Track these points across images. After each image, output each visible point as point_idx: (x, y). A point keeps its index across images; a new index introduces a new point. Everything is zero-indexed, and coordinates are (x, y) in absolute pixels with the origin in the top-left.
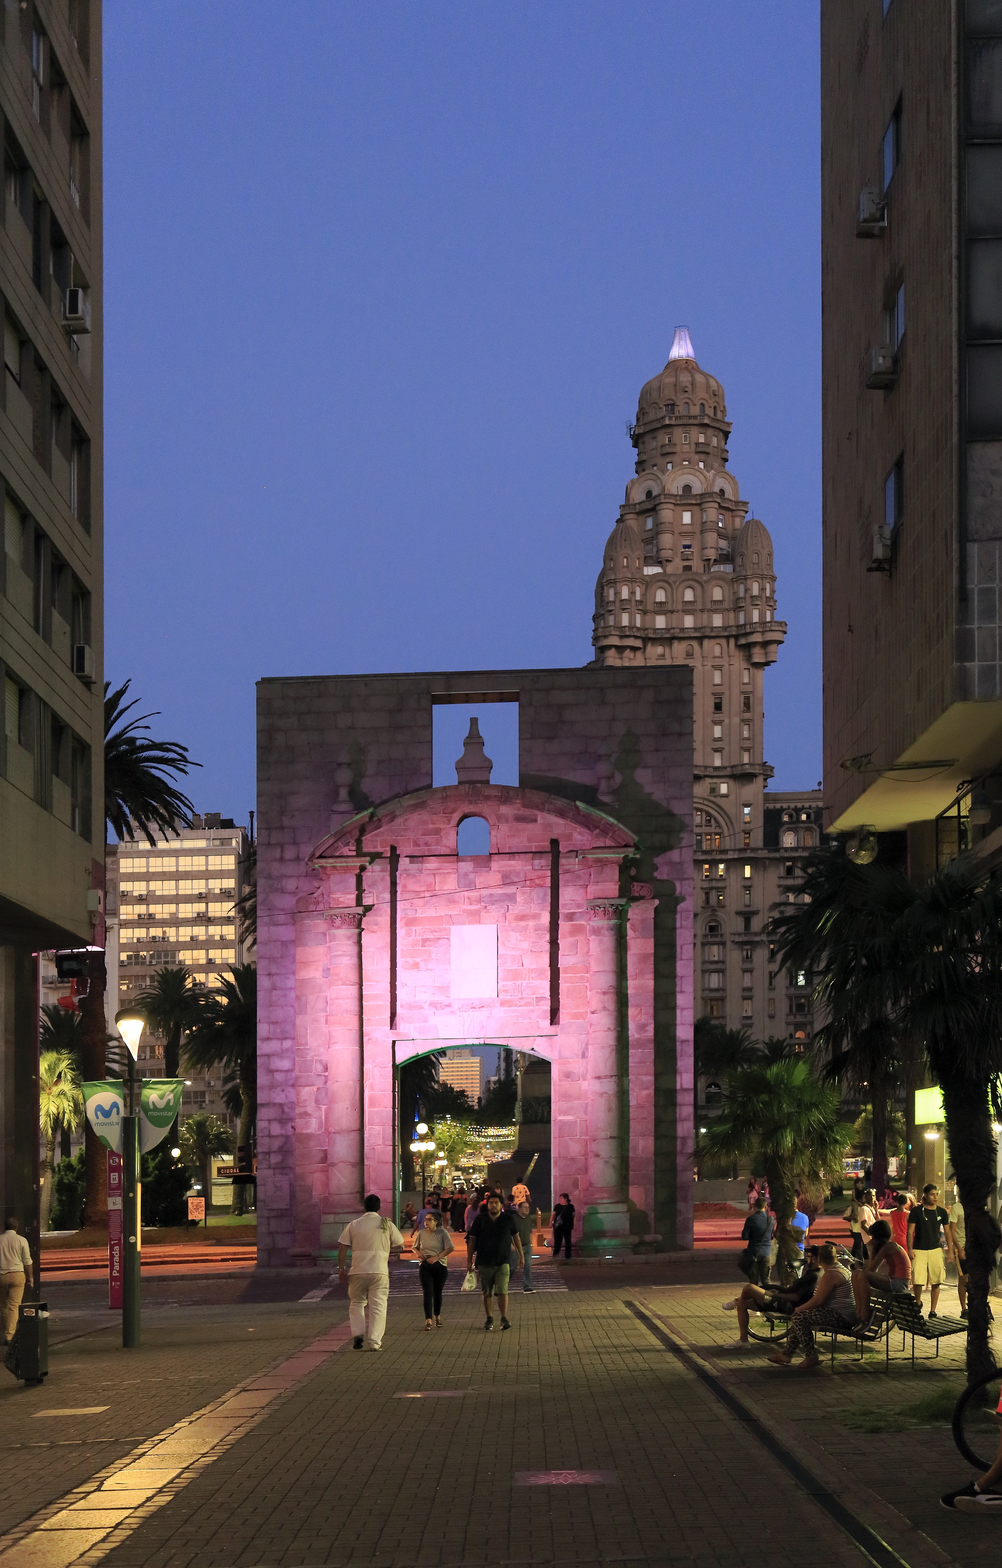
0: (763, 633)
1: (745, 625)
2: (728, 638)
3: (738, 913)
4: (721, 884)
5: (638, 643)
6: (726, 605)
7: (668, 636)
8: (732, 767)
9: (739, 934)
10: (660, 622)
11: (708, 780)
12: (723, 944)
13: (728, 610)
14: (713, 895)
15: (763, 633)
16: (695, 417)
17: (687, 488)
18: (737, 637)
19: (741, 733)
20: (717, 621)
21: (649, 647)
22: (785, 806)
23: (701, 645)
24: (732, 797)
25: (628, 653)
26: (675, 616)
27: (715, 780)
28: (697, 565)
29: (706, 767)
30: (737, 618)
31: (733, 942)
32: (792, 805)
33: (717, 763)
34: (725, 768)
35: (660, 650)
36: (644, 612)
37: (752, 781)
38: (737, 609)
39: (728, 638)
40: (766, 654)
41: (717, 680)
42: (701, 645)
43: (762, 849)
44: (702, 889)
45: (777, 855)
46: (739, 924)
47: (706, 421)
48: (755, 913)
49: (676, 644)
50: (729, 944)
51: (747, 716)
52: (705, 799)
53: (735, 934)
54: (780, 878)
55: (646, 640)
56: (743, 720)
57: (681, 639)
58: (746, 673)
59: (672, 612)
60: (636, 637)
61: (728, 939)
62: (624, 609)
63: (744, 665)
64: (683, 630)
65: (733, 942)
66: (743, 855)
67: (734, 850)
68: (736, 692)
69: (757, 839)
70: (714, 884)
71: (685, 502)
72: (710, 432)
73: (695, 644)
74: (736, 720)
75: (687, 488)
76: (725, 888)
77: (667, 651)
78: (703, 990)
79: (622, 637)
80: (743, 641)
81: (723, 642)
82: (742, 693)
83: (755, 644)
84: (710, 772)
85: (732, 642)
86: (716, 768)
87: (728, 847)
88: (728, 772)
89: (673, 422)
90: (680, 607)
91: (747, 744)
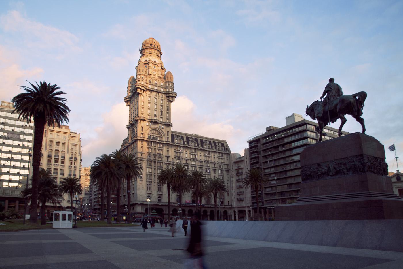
0: (172, 94)
1: (168, 92)
2: (164, 94)
3: (166, 156)
4: (162, 149)
5: (145, 89)
6: (164, 87)
7: (152, 90)
8: (165, 122)
9: (166, 161)
10: (150, 86)
11: (159, 124)
12: (162, 163)
13: (164, 88)
14: (160, 151)
15: (172, 94)
16: (157, 48)
17: (155, 61)
18: (166, 94)
19: (166, 115)
20: (162, 89)
21: (147, 91)
22: (175, 134)
23: (158, 94)
24: (165, 129)
25: (142, 91)
26: (153, 86)
27: (161, 125)
28: (157, 77)
29: (159, 121)
30: (166, 90)
31: (164, 163)
32: (176, 134)
33: (161, 121)
34: (163, 122)
35: (149, 93)
36: (146, 83)
37: (169, 127)
38: (166, 88)
39: (164, 94)
40: (173, 99)
41: (162, 103)
42: (158, 94)
43: (171, 142)
44: (158, 149)
45: (174, 144)
46: (166, 159)
47: (159, 50)
48: (170, 157)
49: (153, 92)
50: (163, 163)
51: (168, 112)
52: (158, 128)
53: (165, 161)
54: (175, 150)
55: (147, 89)
56: (167, 113)
57: (154, 91)
58: (168, 103)
59: (152, 85)
60: (145, 88)
61: (163, 162)
62: (142, 81)
63: (167, 101)
64: (155, 89)
65: (164, 163)
66: (167, 143)
67: (165, 141)
68: (166, 106)
69: (170, 140)
70: (160, 148)
71: (155, 63)
72: (159, 52)
73: (157, 93)
74: (166, 112)
75: (155, 61)
76: (162, 150)
77: (151, 93)
78: (158, 173)
79: (142, 87)
80: (168, 95)
81: (163, 95)
82: (167, 106)
83: (170, 96)
84: (160, 122)
85: (165, 95)
86: (161, 122)
87: (163, 140)
88: (164, 123)
89: (152, 47)
90: (154, 84)
91: (168, 118)
